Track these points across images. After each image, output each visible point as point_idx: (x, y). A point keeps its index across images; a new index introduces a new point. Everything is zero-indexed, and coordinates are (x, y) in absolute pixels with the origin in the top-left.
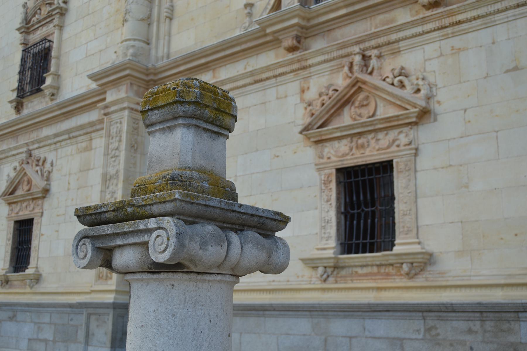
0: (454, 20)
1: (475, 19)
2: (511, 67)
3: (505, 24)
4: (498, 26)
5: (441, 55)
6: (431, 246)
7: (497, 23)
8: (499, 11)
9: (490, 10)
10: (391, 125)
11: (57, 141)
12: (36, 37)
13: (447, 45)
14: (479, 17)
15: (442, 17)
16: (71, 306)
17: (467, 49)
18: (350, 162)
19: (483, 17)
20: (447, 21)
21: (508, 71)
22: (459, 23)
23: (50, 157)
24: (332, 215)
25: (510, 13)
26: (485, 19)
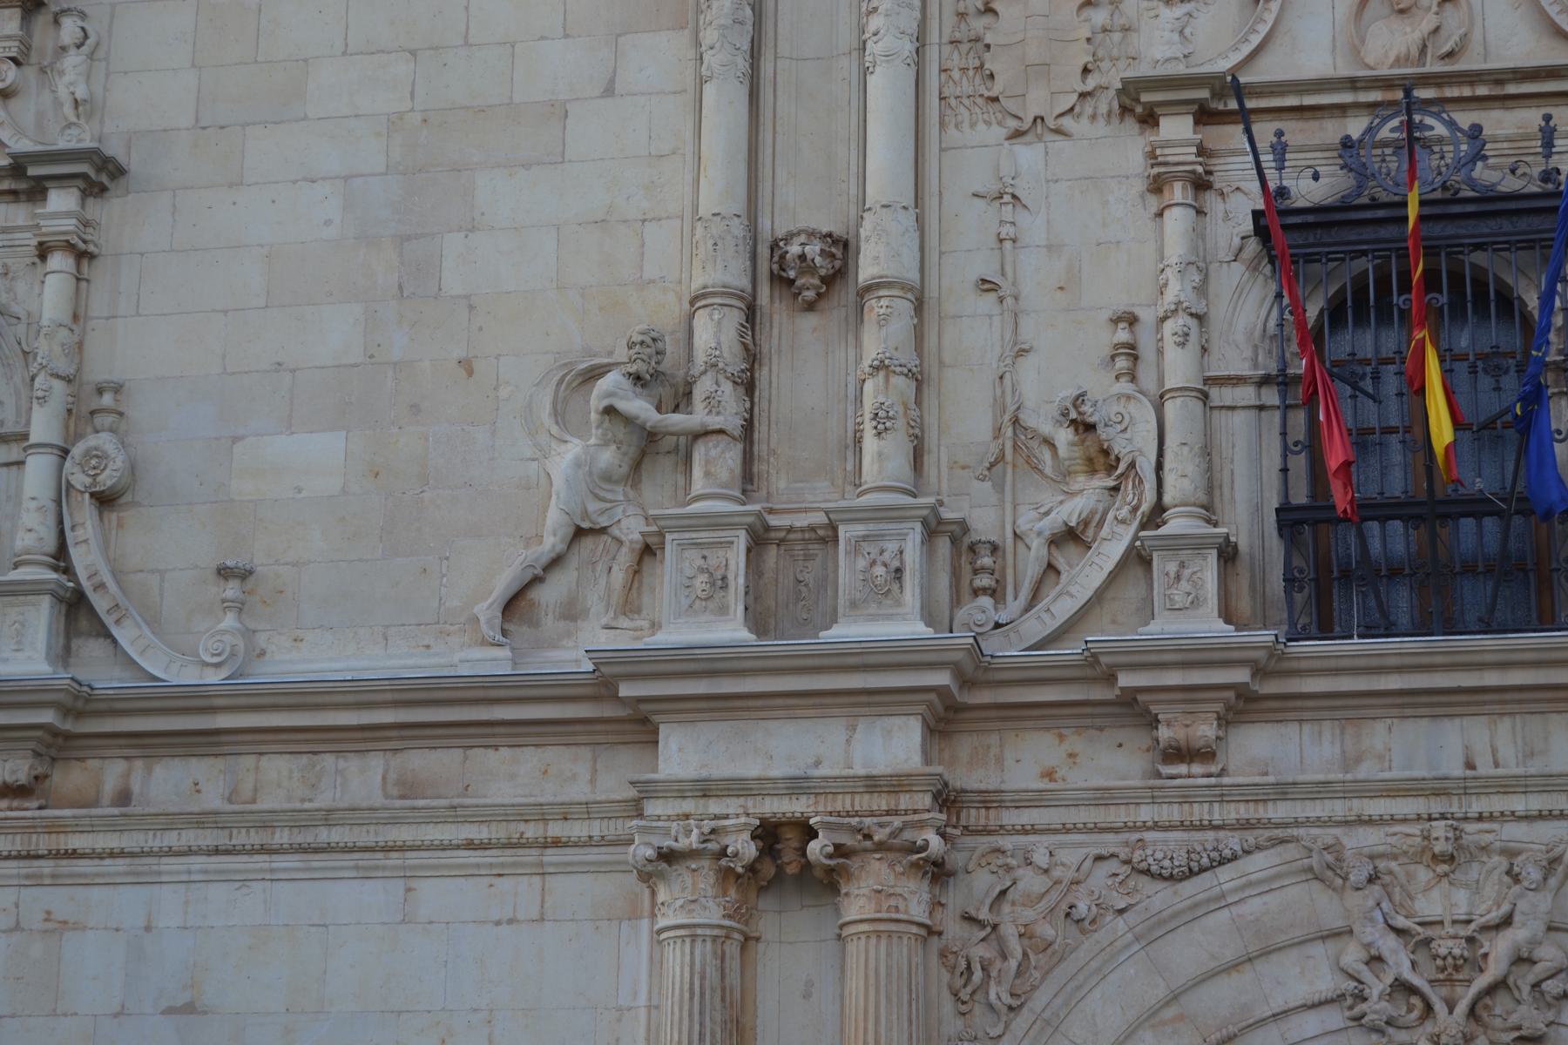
0: (62, 847)
1: (112, 854)
2: (179, 1003)
3: (183, 886)
4: (165, 887)
5: (17, 927)
7: (164, 879)
8: (170, 852)
9: (150, 843)
14: (122, 854)
15: (30, 829)
17: (84, 928)
19: (132, 855)
20: (43, 843)
21: (170, 1011)
22: (73, 854)
25: (198, 862)
26: (137, 861)
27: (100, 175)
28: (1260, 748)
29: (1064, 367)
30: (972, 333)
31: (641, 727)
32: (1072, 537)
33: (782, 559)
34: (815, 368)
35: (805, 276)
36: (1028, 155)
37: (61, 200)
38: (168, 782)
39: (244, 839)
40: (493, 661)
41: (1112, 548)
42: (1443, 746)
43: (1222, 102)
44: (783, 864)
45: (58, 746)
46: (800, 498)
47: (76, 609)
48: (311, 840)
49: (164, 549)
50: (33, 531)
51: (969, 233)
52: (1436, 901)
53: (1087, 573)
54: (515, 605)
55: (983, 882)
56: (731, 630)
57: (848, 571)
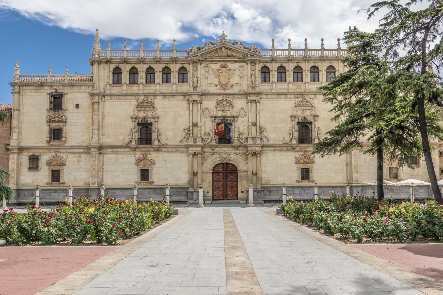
6: (154, 180)
10: (149, 164)
11: (68, 154)
12: (55, 125)
13: (158, 155)
16: (79, 189)
18: (143, 168)
23: (65, 157)
24: (140, 176)
27: (158, 118)
28: (217, 149)
29: (208, 130)
30: (203, 128)
31: (188, 148)
32: (208, 139)
33: (195, 140)
34: (195, 130)
35: (195, 125)
36: (206, 119)
37: (156, 119)
38: (164, 149)
39: (168, 152)
40: (180, 144)
41: (210, 139)
42: (224, 149)
43: (215, 117)
44: (195, 154)
45: (158, 148)
46: (195, 136)
47: (159, 141)
48: (171, 152)
49: (162, 138)
50: (156, 137)
51: (203, 123)
52: (224, 156)
53: (209, 141)
54: (181, 141)
55: (204, 155)
56: (192, 143)
57: (198, 140)
